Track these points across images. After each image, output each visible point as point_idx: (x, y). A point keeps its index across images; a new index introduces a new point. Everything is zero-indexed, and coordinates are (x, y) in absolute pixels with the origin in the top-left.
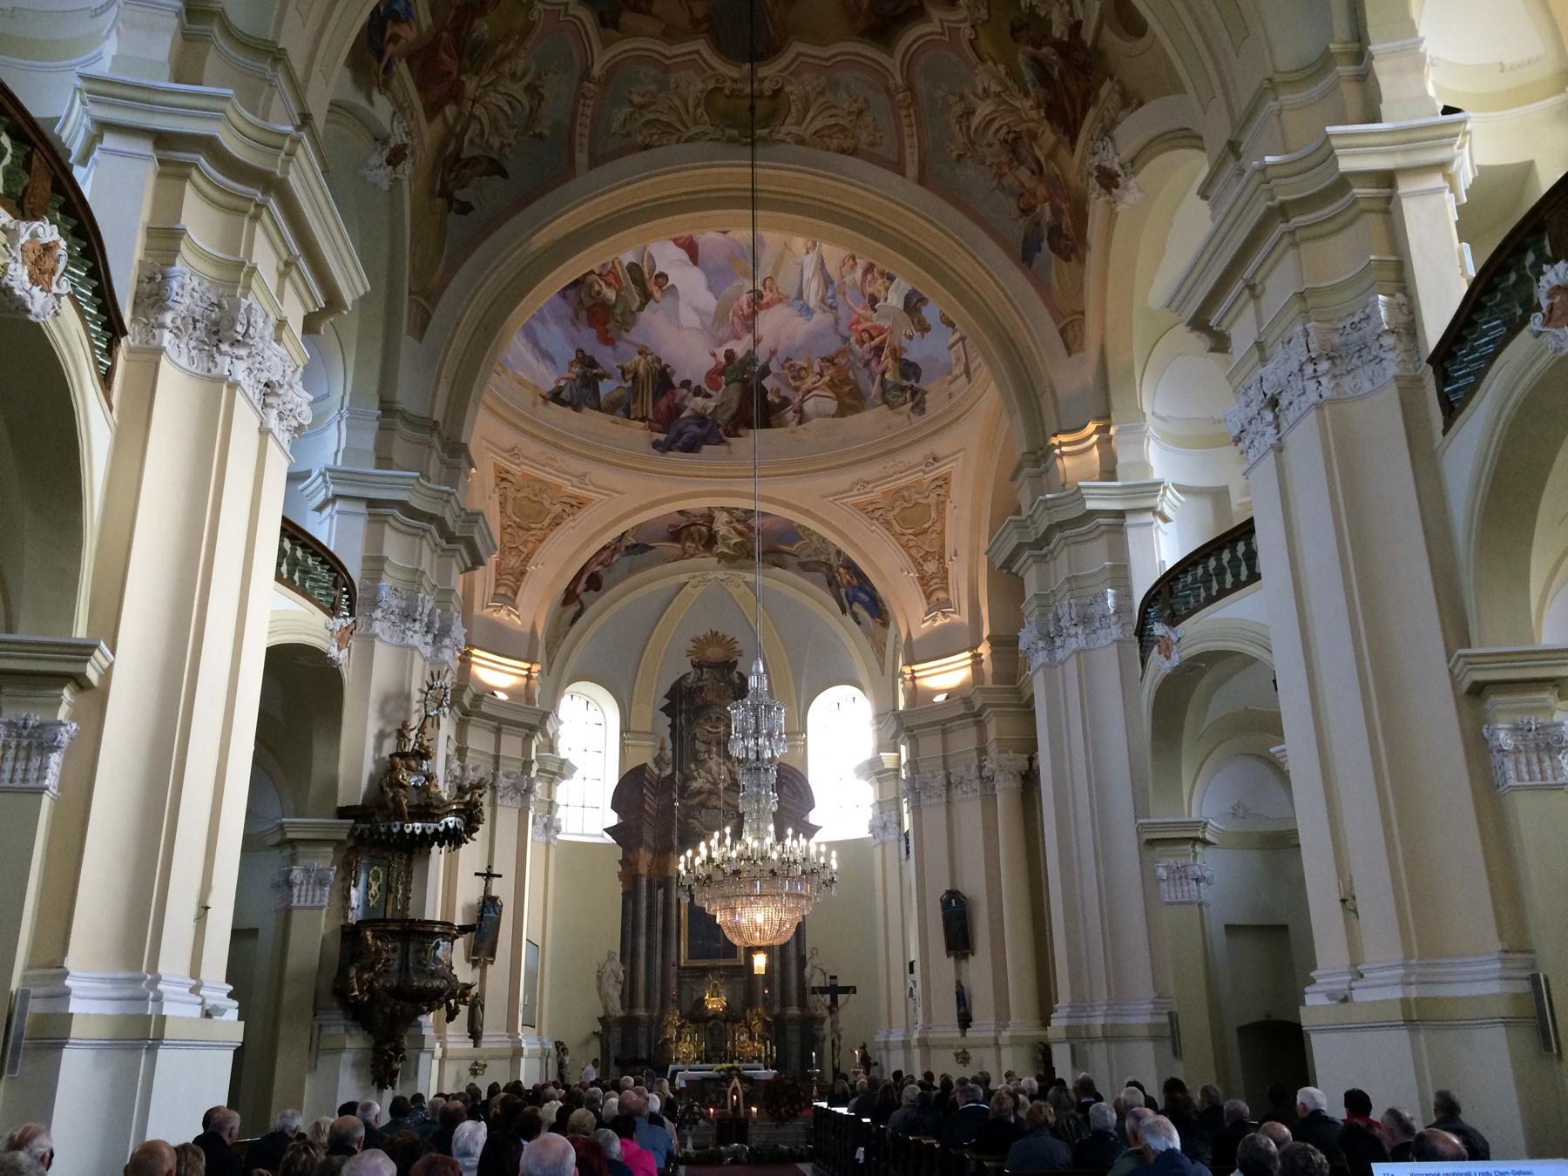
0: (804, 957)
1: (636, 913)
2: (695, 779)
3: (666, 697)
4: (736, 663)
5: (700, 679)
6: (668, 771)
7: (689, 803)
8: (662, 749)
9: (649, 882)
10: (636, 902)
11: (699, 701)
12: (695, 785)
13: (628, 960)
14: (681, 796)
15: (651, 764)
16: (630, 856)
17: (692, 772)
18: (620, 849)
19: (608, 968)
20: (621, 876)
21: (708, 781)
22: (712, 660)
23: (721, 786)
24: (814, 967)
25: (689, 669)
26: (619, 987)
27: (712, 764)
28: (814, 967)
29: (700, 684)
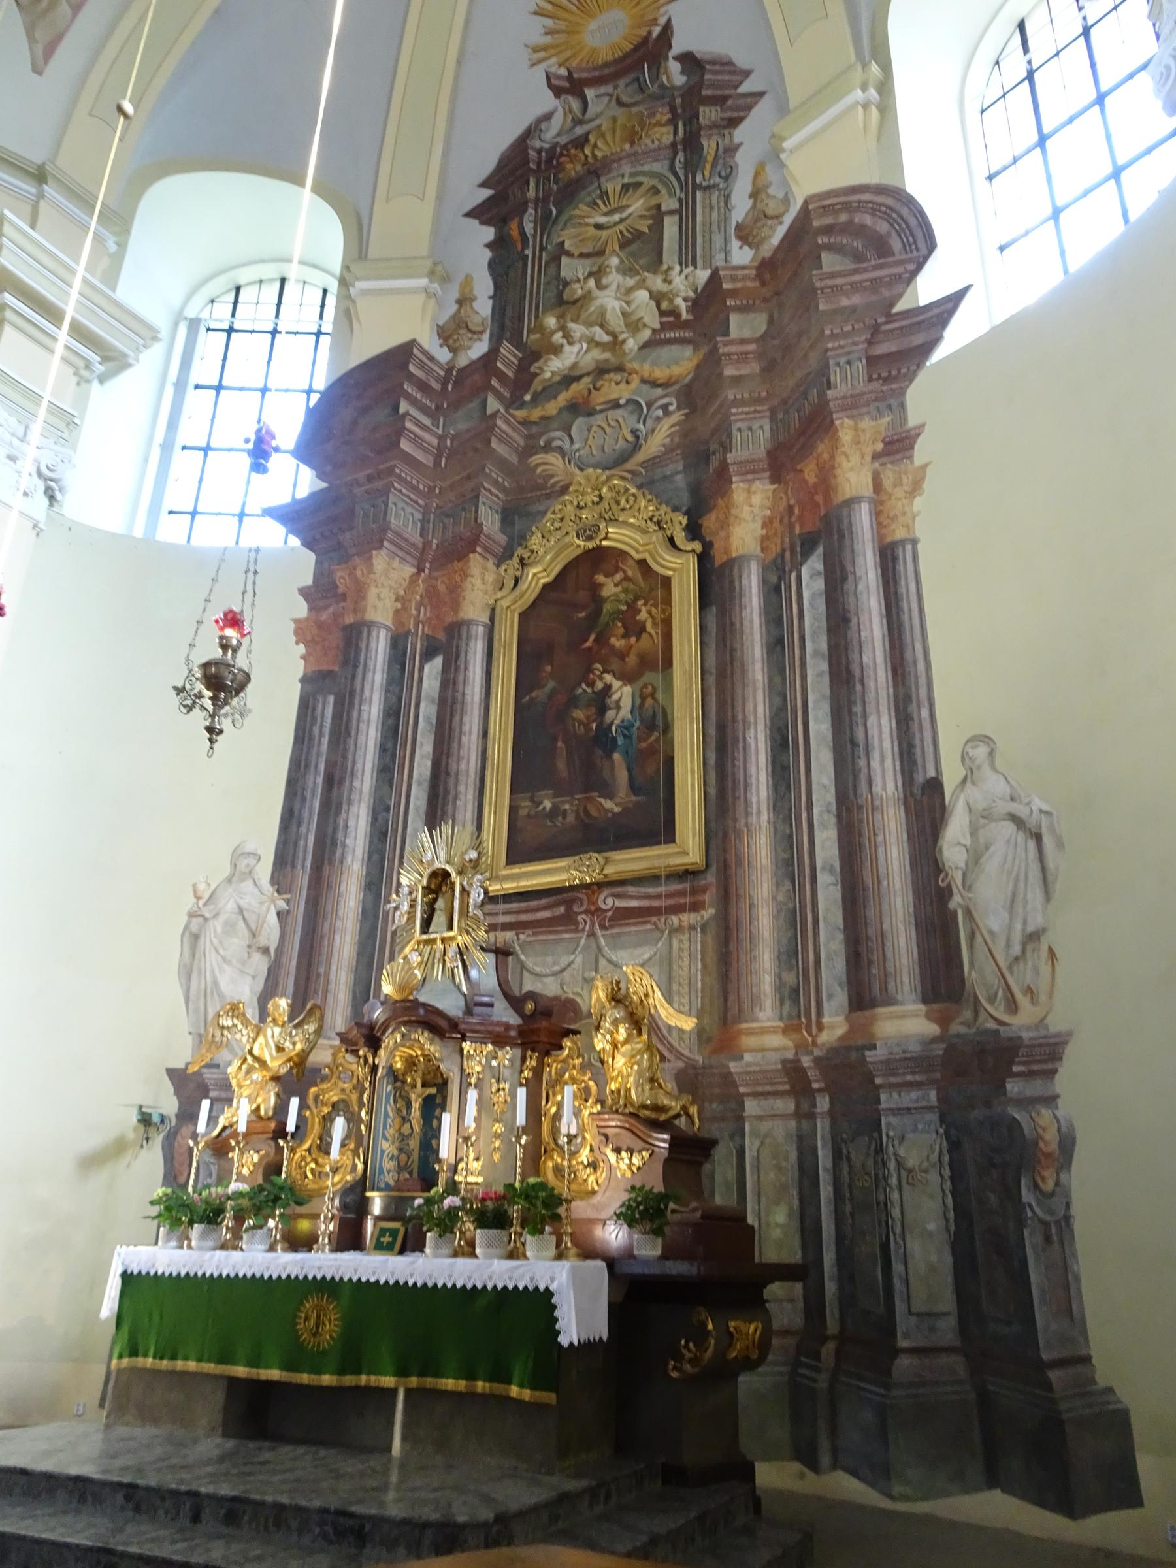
0: (935, 785)
1: (343, 732)
2: (557, 350)
3: (483, 185)
4: (668, 28)
5: (577, 122)
6: (479, 349)
7: (536, 414)
8: (464, 301)
9: (398, 644)
10: (346, 704)
11: (573, 169)
12: (554, 366)
13: (303, 877)
14: (514, 402)
15: (429, 341)
16: (341, 576)
17: (547, 335)
18: (311, 557)
19: (228, 905)
20: (301, 631)
21: (593, 343)
22: (605, 56)
23: (631, 344)
24: (981, 818)
25: (547, 101)
26: (260, 964)
27: (609, 302)
28: (981, 818)
29: (579, 131)
